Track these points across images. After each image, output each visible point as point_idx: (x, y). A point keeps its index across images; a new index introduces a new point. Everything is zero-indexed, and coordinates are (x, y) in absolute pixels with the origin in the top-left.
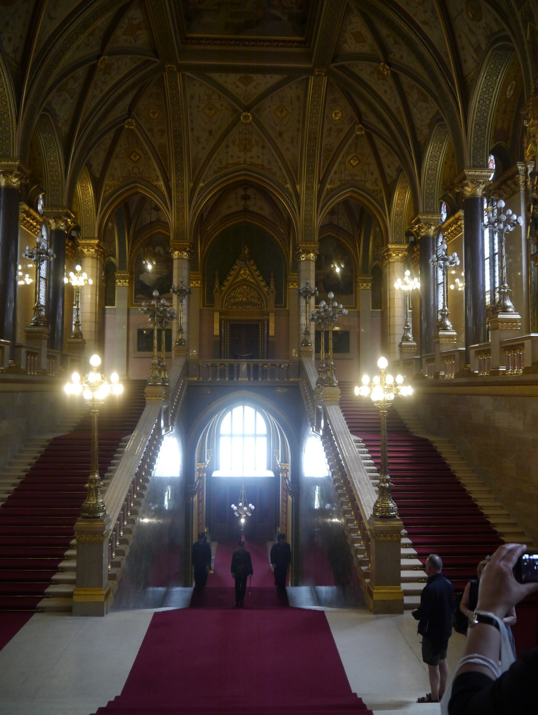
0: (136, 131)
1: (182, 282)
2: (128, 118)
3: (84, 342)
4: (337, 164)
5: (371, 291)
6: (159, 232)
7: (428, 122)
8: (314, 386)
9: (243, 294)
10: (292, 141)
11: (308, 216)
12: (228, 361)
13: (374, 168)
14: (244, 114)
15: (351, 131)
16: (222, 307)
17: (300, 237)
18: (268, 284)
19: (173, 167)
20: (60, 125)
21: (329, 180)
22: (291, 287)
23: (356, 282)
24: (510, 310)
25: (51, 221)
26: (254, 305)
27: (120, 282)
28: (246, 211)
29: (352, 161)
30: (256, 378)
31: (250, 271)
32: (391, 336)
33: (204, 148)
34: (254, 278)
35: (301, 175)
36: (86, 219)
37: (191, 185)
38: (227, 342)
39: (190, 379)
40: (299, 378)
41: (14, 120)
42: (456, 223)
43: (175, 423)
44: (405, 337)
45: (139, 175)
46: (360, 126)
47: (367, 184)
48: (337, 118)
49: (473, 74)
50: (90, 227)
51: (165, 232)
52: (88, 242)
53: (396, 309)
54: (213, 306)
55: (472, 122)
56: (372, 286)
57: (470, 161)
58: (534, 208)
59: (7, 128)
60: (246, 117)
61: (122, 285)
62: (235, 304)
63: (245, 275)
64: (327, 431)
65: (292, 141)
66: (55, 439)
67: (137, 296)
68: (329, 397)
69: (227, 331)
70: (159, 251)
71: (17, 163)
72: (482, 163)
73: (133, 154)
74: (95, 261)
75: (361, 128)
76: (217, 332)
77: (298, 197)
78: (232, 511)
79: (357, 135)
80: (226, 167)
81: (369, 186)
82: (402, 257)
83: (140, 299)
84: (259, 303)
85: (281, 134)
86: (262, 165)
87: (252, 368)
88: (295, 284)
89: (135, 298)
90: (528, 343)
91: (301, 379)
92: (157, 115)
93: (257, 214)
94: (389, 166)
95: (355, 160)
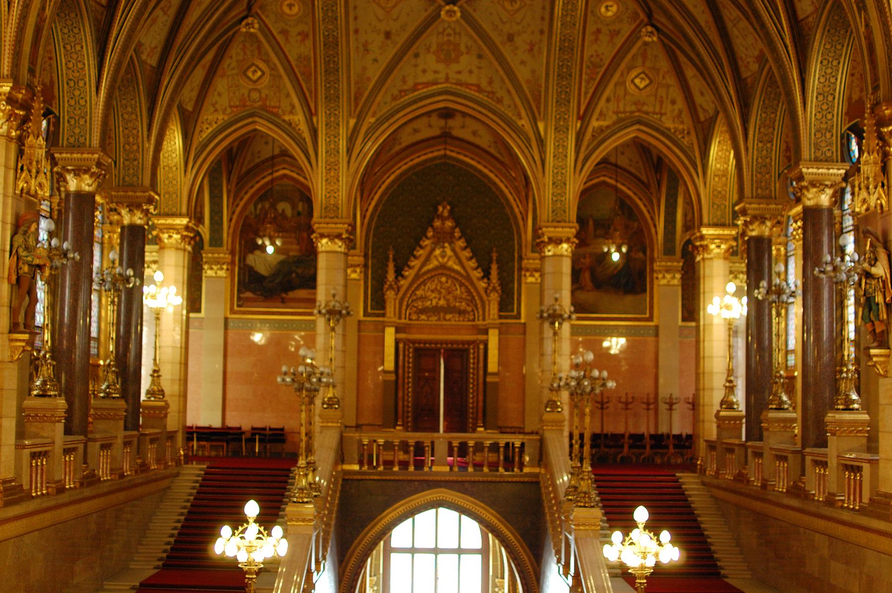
1: (334, 296)
2: (246, 17)
3: (167, 406)
4: (611, 86)
5: (680, 289)
6: (285, 176)
7: (756, 53)
8: (562, 497)
9: (440, 293)
10: (531, 50)
12: (413, 437)
13: (675, 92)
14: (447, 8)
15: (634, 36)
16: (400, 318)
17: (545, 213)
18: (487, 275)
19: (321, 95)
20: (144, 57)
21: (597, 111)
22: (531, 280)
23: (652, 271)
24: (856, 406)
25: (124, 212)
26: (461, 312)
27: (212, 269)
28: (446, 137)
30: (463, 466)
31: (453, 250)
32: (706, 393)
33: (376, 60)
35: (546, 106)
36: (167, 182)
37: (352, 122)
38: (409, 383)
39: (347, 467)
40: (539, 466)
41: (94, 89)
43: (328, 557)
44: (726, 401)
45: (260, 103)
46: (650, 29)
47: (664, 119)
48: (610, 14)
49: (811, 19)
50: (174, 196)
51: (294, 175)
52: (170, 221)
53: (715, 344)
54: (384, 315)
55: (813, 91)
56: (682, 278)
57: (810, 150)
58: (866, 283)
59: (82, 102)
60: (451, 13)
61: (216, 274)
62: (424, 311)
63: (443, 257)
65: (531, 50)
66: (141, 584)
67: (242, 295)
68: (584, 525)
69: (409, 363)
70: (283, 210)
71: (96, 156)
72: (829, 154)
73: (252, 69)
74: (181, 253)
75: (652, 33)
77: (541, 143)
79: (646, 44)
80: (415, 88)
81: (668, 123)
82: (727, 251)
83: (248, 300)
84: (469, 309)
85: (510, 38)
86: (478, 86)
87: (456, 449)
88: (537, 275)
89: (239, 299)
90: (866, 467)
91: (543, 471)
92: (295, 9)
93: (468, 143)
94: (702, 94)
95: (642, 79)
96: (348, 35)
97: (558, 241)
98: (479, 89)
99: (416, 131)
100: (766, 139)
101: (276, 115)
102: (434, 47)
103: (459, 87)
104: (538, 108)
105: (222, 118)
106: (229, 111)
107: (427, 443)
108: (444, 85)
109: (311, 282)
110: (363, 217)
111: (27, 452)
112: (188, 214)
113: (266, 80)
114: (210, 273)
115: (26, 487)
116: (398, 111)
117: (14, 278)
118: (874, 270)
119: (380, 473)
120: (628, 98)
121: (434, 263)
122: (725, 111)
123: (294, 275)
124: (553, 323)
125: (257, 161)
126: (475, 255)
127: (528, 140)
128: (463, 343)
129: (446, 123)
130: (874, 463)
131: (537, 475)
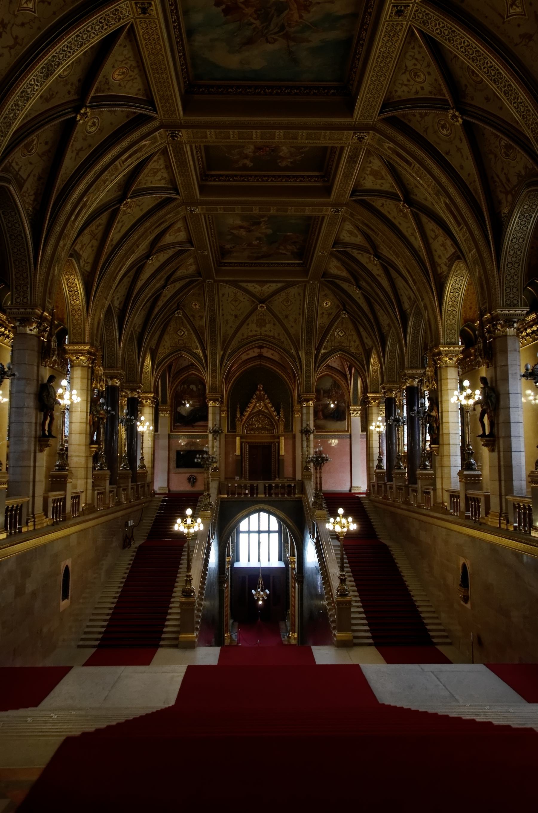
0: (183, 318)
3: (147, 471)
6: (193, 374)
8: (311, 507)
13: (355, 337)
18: (278, 414)
28: (260, 356)
30: (270, 495)
34: (268, 409)
37: (222, 353)
39: (222, 496)
46: (344, 312)
54: (235, 432)
64: (317, 539)
66: (140, 546)
76: (238, 452)
78: (252, 595)
79: (343, 318)
80: (247, 338)
81: (353, 350)
85: (287, 317)
90: (432, 492)
92: (198, 306)
94: (367, 338)
96: (220, 316)
97: (307, 401)
99: (248, 354)
100: (392, 358)
101: (190, 350)
102: (255, 321)
105: (167, 351)
107: (255, 485)
109: (206, 419)
110: (226, 391)
111: (96, 492)
112: (154, 392)
113: (186, 334)
114: (162, 415)
115: (96, 506)
116: (241, 348)
117: (92, 423)
118: (431, 413)
119: (236, 498)
122: (376, 346)
124: (306, 435)
125: (181, 367)
126: (274, 406)
127: (295, 359)
128: (269, 443)
130: (435, 490)
131: (301, 498)
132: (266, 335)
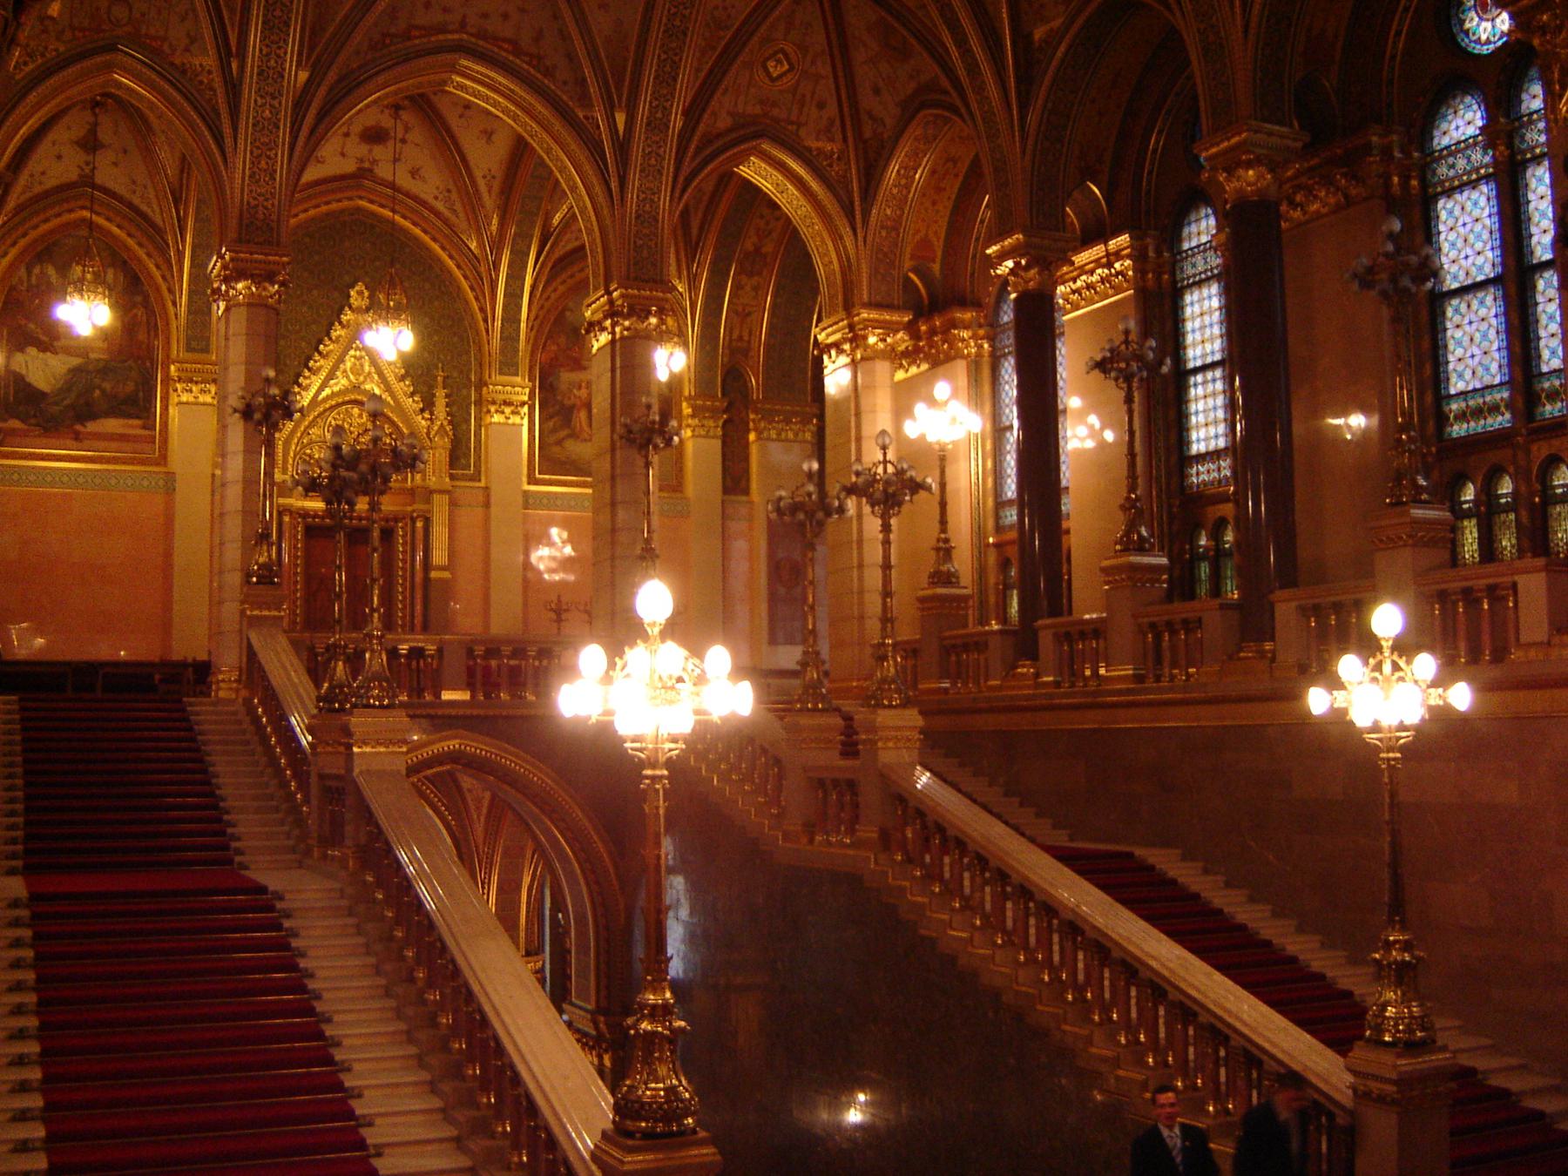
6: (84, 220)
11: (647, 207)
18: (428, 405)
22: (497, 418)
28: (362, 175)
29: (771, 64)
42: (1110, 265)
83: (13, 432)
94: (877, 91)
95: (779, 62)
98: (517, 50)
103: (481, 43)
104: (619, 87)
106: (68, 35)
108: (456, 36)
120: (753, 90)
121: (340, 383)
123: (97, 393)
129: (370, 151)
132: (482, 35)
